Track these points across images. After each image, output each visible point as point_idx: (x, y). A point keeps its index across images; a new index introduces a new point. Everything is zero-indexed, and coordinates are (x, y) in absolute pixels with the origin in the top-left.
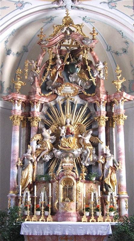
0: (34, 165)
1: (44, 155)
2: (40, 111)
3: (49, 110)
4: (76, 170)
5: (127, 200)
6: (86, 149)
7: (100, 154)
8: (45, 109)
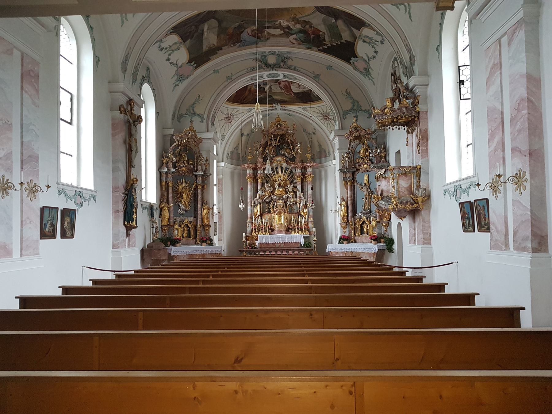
0: (261, 205)
1: (266, 199)
4: (284, 207)
5: (313, 223)
7: (298, 197)
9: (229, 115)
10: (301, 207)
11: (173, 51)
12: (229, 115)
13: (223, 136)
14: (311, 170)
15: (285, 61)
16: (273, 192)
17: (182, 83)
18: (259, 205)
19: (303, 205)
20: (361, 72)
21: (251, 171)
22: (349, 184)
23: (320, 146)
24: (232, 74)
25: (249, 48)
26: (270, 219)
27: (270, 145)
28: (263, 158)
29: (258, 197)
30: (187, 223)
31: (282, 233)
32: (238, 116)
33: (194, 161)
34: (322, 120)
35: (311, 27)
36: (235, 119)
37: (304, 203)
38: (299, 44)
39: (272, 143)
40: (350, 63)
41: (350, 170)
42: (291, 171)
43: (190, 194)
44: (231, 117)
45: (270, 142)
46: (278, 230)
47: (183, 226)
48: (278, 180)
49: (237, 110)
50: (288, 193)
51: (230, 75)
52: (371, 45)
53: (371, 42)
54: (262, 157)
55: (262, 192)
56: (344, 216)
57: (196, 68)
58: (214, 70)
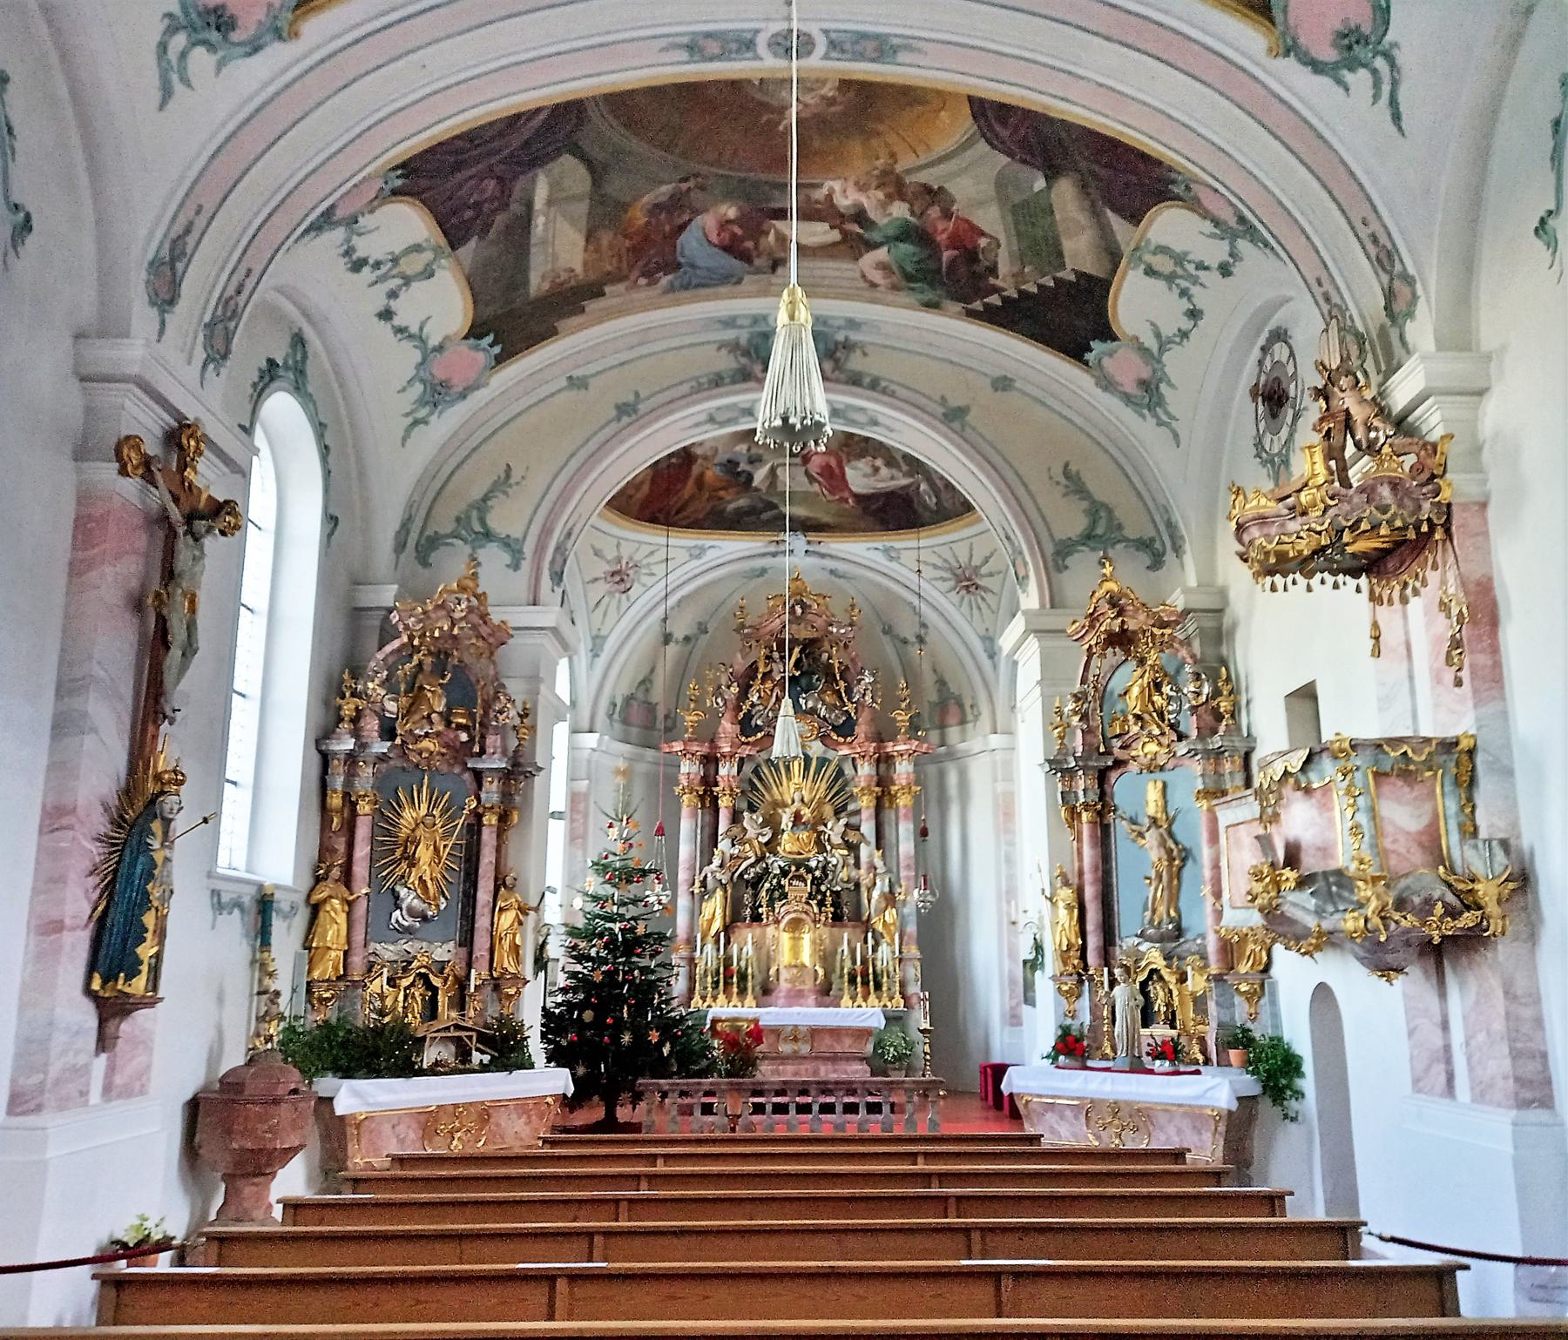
0: (726, 891)
2: (739, 772)
3: (756, 772)
6: (833, 856)
8: (748, 768)
9: (624, 563)
10: (873, 901)
12: (624, 563)
13: (598, 641)
14: (911, 768)
16: (772, 846)
18: (719, 893)
19: (883, 894)
20: (1128, 399)
21: (695, 769)
22: (1085, 816)
23: (942, 683)
24: (637, 394)
25: (707, 298)
26: (758, 946)
27: (767, 676)
28: (740, 723)
29: (716, 861)
30: (423, 970)
31: (802, 1001)
32: (655, 569)
33: (471, 716)
34: (954, 593)
35: (947, 214)
36: (645, 579)
37: (887, 889)
38: (895, 288)
39: (771, 671)
40: (1086, 363)
41: (1091, 763)
42: (840, 773)
43: (445, 846)
44: (631, 572)
45: (766, 665)
46: (789, 991)
47: (405, 983)
48: (793, 802)
49: (653, 548)
50: (829, 848)
51: (631, 398)
52: (1177, 285)
53: (1179, 271)
54: (736, 716)
55: (733, 845)
56: (1070, 946)
57: (500, 360)
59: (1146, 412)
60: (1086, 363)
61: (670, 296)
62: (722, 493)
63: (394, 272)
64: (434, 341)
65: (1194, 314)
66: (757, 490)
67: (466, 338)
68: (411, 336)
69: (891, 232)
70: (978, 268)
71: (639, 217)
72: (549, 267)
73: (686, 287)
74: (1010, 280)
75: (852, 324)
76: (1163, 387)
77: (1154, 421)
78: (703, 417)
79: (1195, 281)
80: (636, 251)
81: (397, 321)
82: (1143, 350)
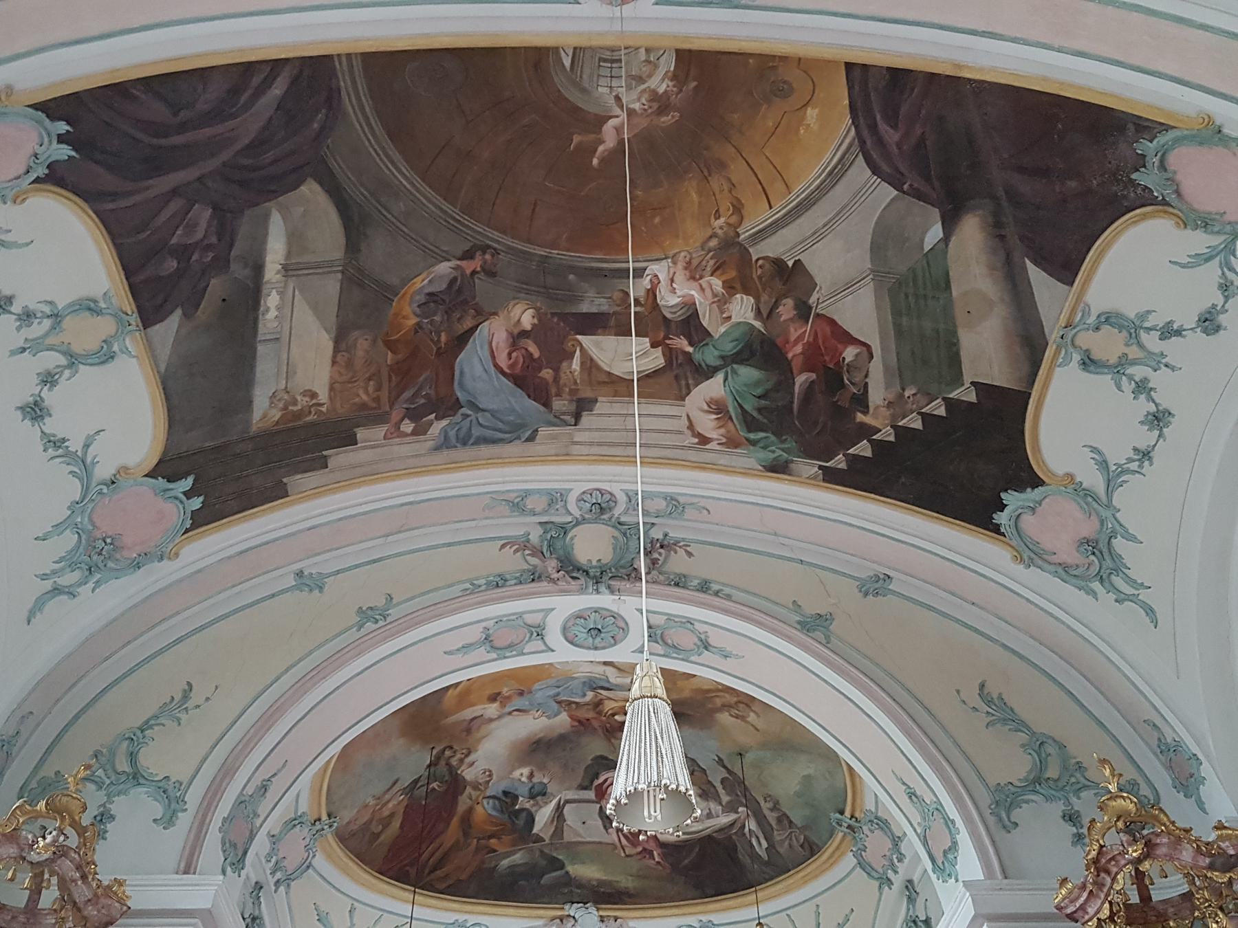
11: (74, 360)
15: (655, 555)
17: (98, 583)
20: (1066, 571)
24: (390, 597)
25: (491, 462)
35: (804, 311)
38: (732, 443)
40: (996, 529)
51: (381, 602)
52: (1131, 378)
53: (1134, 352)
57: (200, 520)
58: (300, 574)
59: (1096, 585)
60: (996, 529)
61: (445, 454)
62: (493, 841)
63: (51, 340)
64: (103, 471)
65: (1159, 419)
66: (539, 839)
67: (151, 475)
68: (68, 454)
69: (729, 348)
70: (843, 400)
71: (407, 314)
72: (282, 385)
73: (465, 441)
74: (885, 412)
75: (675, 505)
76: (1119, 543)
77: (1112, 596)
78: (475, 634)
79: (1157, 361)
80: (403, 374)
81: (50, 426)
82: (1083, 494)
